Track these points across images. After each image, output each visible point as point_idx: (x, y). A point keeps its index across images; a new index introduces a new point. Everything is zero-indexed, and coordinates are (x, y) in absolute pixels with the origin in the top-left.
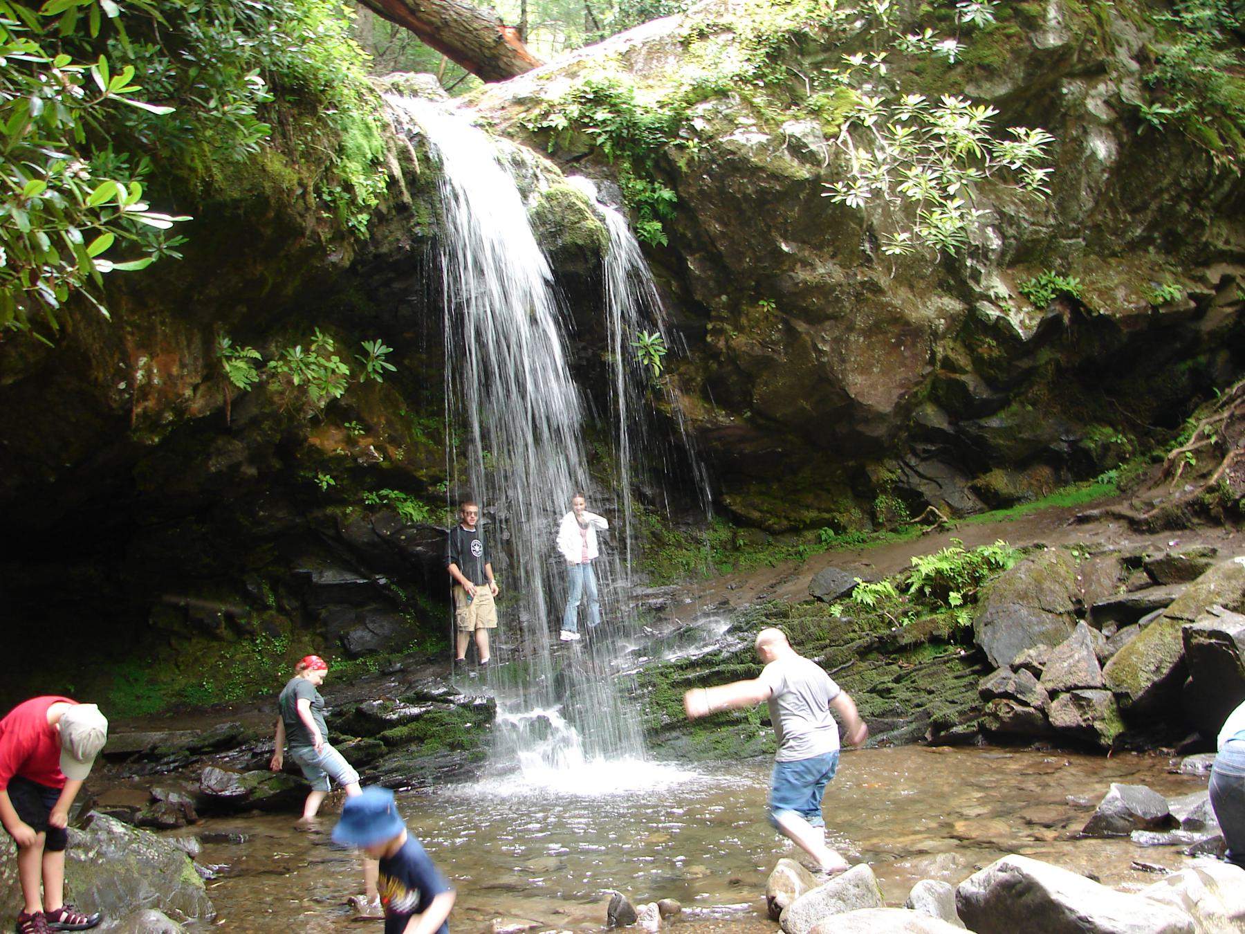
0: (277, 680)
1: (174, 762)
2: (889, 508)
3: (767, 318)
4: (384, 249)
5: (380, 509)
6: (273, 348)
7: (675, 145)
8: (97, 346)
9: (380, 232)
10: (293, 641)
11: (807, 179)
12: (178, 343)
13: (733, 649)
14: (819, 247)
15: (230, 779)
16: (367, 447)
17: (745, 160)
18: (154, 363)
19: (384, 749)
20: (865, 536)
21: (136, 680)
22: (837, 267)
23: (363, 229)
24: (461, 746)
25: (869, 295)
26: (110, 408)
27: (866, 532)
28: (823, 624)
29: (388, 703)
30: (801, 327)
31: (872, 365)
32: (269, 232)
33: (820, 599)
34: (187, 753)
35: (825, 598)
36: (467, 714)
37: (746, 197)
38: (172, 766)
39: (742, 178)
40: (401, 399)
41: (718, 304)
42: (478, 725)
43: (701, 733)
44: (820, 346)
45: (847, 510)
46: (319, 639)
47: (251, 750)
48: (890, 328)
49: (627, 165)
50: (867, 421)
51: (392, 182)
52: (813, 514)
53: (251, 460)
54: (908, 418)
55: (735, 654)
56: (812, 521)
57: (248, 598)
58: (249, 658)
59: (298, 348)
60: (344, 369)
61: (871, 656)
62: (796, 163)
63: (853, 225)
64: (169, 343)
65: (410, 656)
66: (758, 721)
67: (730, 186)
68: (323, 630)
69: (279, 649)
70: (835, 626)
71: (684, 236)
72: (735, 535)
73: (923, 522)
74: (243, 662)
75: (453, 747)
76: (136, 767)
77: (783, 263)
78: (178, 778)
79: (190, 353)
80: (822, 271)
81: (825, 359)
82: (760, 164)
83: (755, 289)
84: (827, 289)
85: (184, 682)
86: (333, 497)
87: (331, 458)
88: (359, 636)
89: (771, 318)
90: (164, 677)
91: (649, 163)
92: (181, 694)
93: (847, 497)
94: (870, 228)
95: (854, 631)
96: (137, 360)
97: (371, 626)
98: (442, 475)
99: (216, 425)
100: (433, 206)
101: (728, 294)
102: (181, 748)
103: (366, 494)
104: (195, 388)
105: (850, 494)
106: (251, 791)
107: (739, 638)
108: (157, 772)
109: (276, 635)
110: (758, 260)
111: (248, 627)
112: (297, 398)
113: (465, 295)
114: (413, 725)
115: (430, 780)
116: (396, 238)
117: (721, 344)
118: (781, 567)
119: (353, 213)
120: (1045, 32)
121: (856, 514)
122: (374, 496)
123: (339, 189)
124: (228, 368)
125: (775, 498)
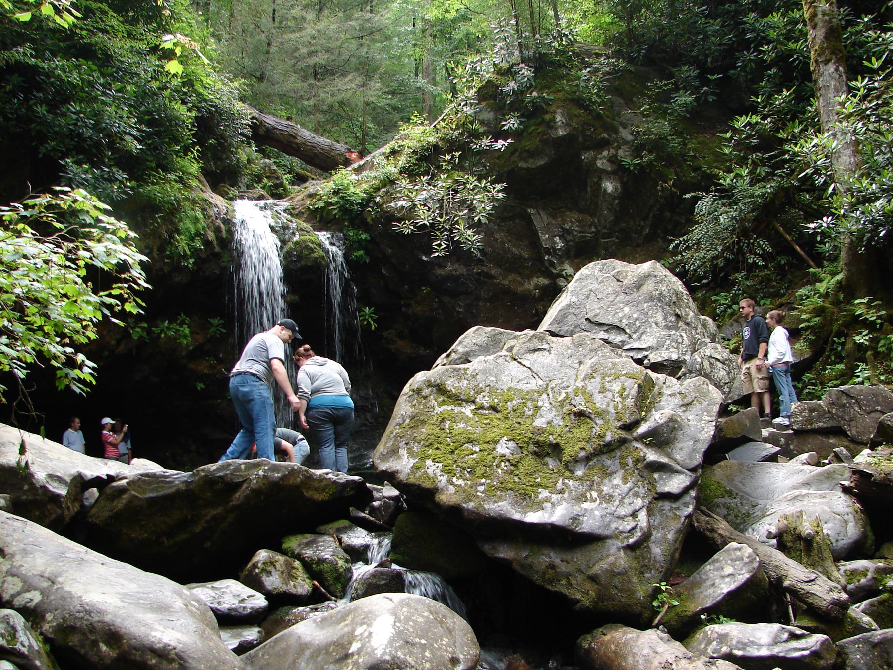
4: (207, 274)
30: (446, 299)
120: (556, 129)
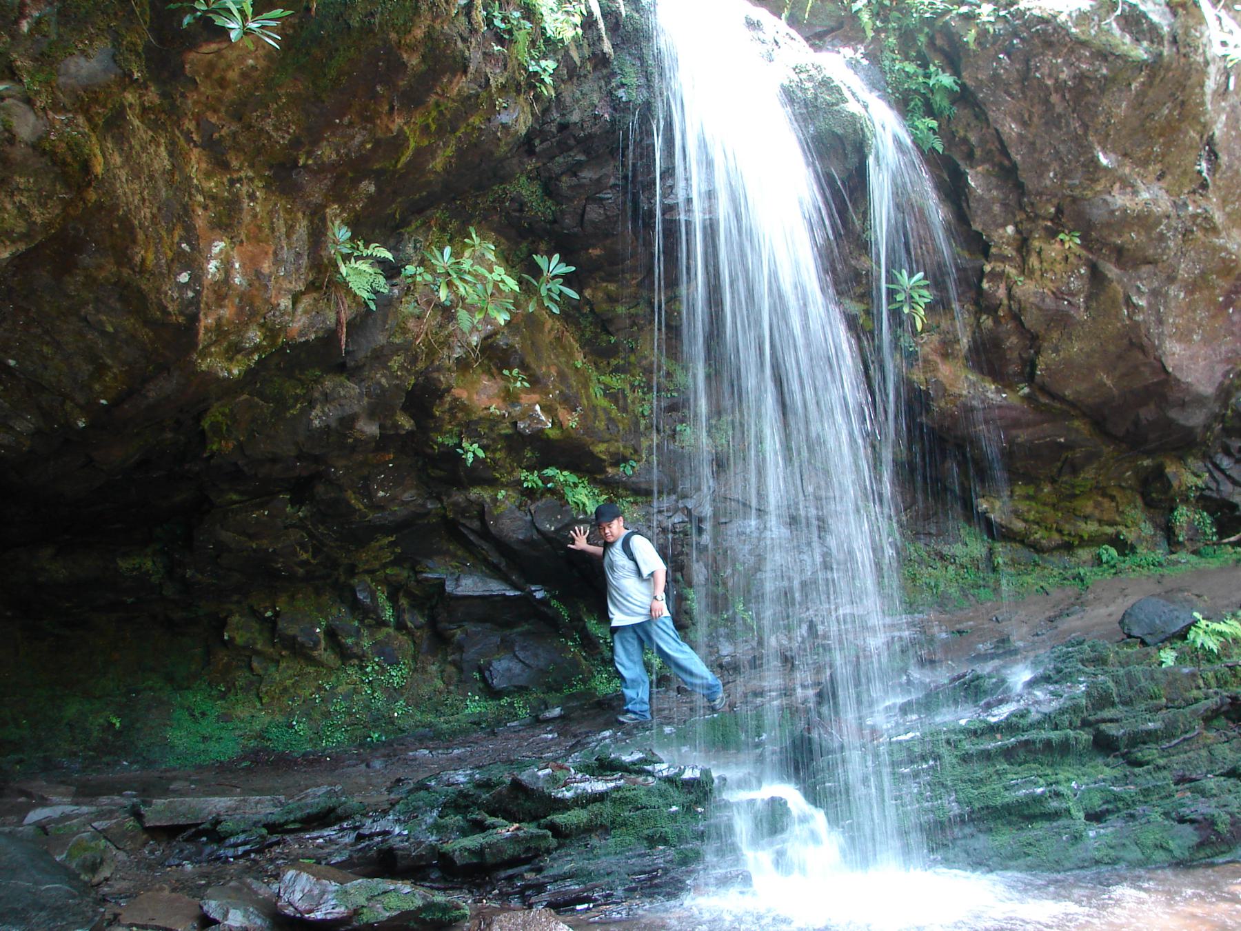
0: (393, 723)
1: (245, 843)
2: (1190, 522)
3: (1066, 258)
4: (575, 117)
5: (542, 495)
6: (410, 249)
7: (959, 15)
8: (146, 212)
9: (568, 91)
10: (415, 670)
11: (1144, 61)
12: (273, 230)
13: (1045, 709)
14: (1144, 163)
15: (323, 893)
16: (532, 406)
17: (1061, 28)
18: (235, 253)
19: (553, 842)
20: (1162, 559)
21: (203, 714)
22: (1162, 193)
23: (548, 80)
24: (664, 840)
25: (1199, 234)
26: (164, 310)
27: (1160, 554)
28: (1158, 675)
29: (559, 774)
31: (1192, 331)
32: (414, 61)
33: (1143, 643)
34: (264, 831)
35: (1148, 639)
36: (672, 791)
37: (1060, 87)
38: (241, 850)
39: (1055, 56)
40: (577, 346)
41: (1002, 237)
42: (688, 809)
43: (1006, 830)
44: (1135, 299)
45: (1135, 524)
46: (451, 669)
47: (355, 828)
48: (1221, 282)
49: (892, 40)
50: (1183, 405)
51: (588, 23)
52: (1091, 528)
53: (372, 414)
54: (1225, 405)
55: (1047, 717)
56: (1090, 536)
57: (356, 607)
58: (355, 691)
59: (448, 250)
60: (512, 284)
61: (1216, 723)
62: (1128, 39)
63: (1192, 133)
64: (260, 228)
65: (571, 697)
66: (1082, 815)
67: (1037, 69)
68: (457, 657)
69: (396, 680)
70: (1172, 678)
71: (965, 140)
72: (991, 552)
73: (1233, 544)
74: (347, 697)
75: (652, 841)
76: (190, 848)
77: (1098, 180)
78: (247, 870)
79: (289, 244)
80: (1145, 195)
81: (1139, 318)
82: (1083, 38)
83: (1056, 218)
84: (1151, 220)
85: (268, 719)
86: (482, 475)
87: (480, 418)
88: (504, 668)
89: (1072, 259)
90: (242, 711)
91: (922, 39)
92: (261, 736)
93: (1136, 507)
94: (1210, 142)
95: (1198, 688)
96: (210, 245)
97: (521, 655)
98: (628, 452)
99: (325, 355)
100: (641, 59)
101: (1016, 226)
102: (255, 824)
103: (524, 473)
104: (296, 299)
105: (1139, 502)
106: (357, 912)
107: (1052, 693)
108: (218, 858)
109: (394, 662)
110: (1065, 174)
111: (355, 650)
112: (441, 326)
113: (681, 195)
114: (595, 808)
115: (620, 892)
116: (587, 104)
117: (1001, 292)
118: (1056, 594)
119: (532, 58)
121: (1147, 529)
122: (536, 479)
123: (517, 14)
124: (343, 270)
125: (1045, 504)
